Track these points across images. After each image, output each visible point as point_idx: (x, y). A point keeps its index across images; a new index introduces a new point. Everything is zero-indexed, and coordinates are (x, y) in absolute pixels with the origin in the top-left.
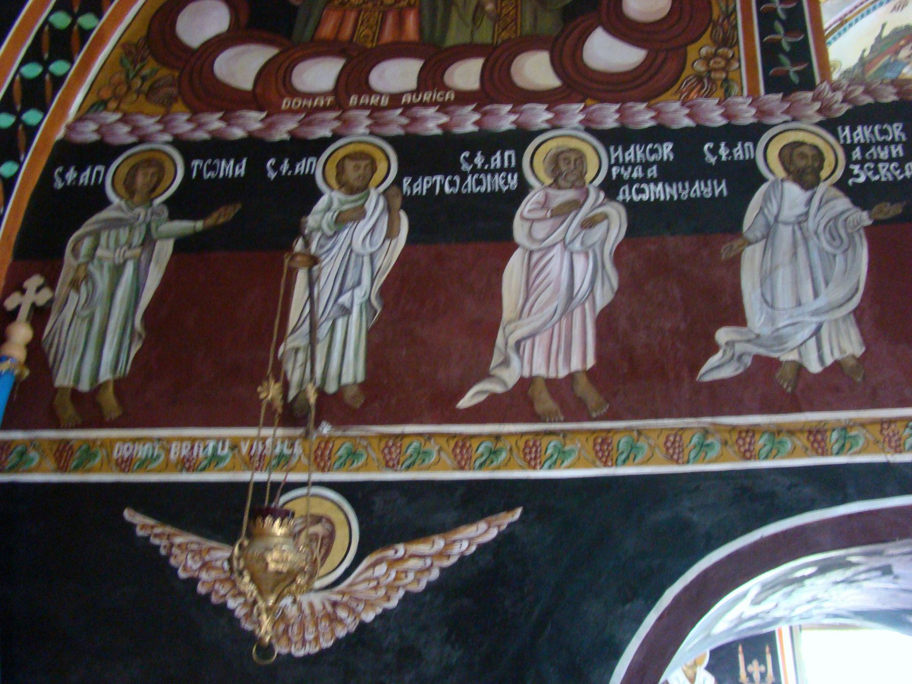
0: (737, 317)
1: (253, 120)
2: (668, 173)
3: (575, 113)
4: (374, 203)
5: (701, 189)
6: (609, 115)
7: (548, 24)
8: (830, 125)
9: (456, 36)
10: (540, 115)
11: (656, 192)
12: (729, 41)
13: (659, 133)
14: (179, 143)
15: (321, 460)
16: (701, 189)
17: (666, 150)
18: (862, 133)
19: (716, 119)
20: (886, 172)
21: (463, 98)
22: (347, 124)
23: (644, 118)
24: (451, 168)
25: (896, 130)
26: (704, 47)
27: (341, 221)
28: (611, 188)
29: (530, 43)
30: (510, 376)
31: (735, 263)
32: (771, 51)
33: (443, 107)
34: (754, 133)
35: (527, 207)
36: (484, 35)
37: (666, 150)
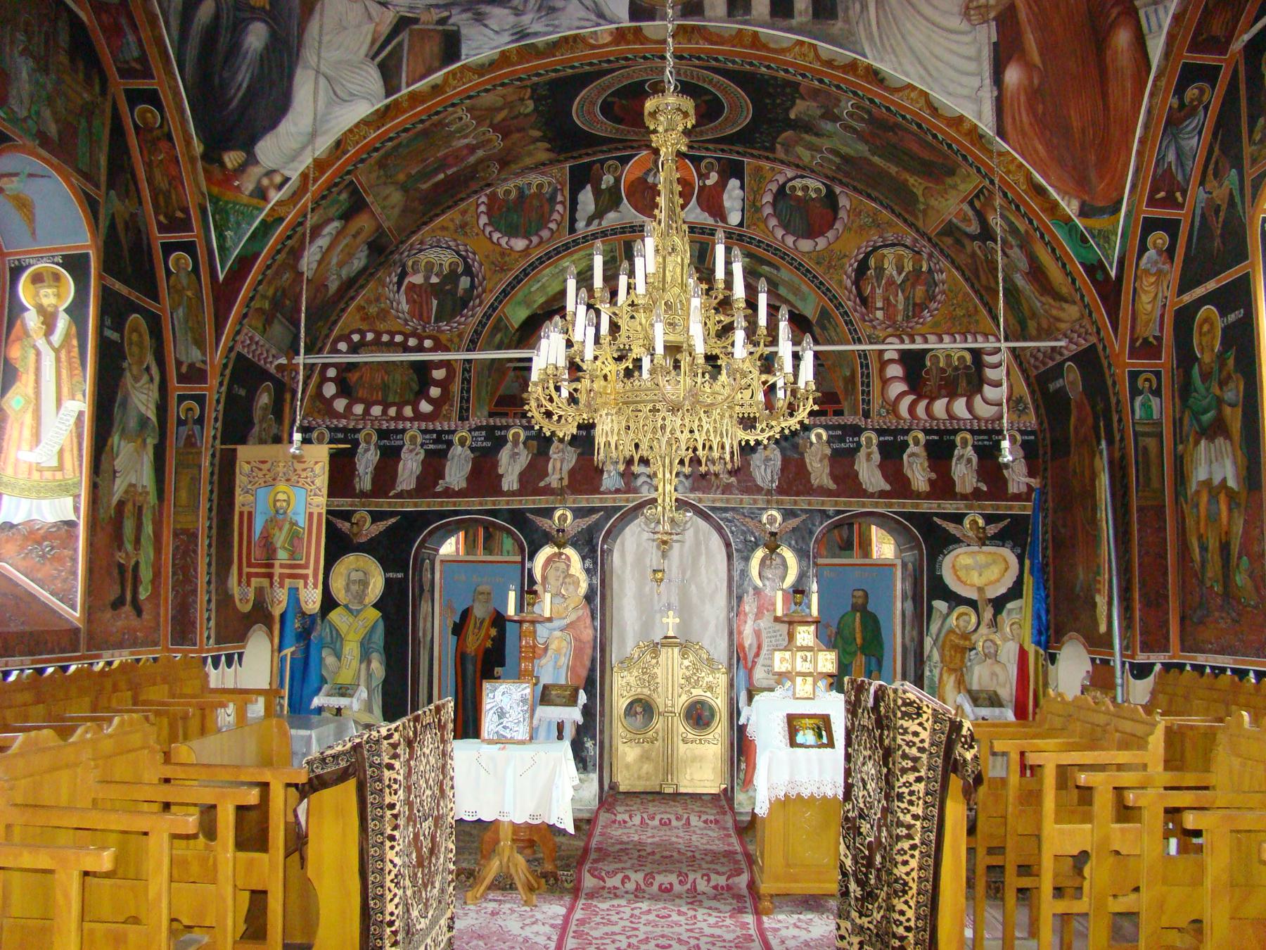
0: (443, 477)
1: (344, 422)
2: (435, 442)
3: (416, 423)
4: (372, 447)
5: (440, 447)
6: (423, 425)
7: (412, 397)
8: (470, 431)
9: (390, 399)
10: (408, 425)
11: (431, 447)
12: (452, 406)
13: (434, 431)
14: (327, 427)
15: (364, 505)
16: (440, 447)
17: (435, 436)
18: (477, 433)
19: (446, 428)
20: (479, 444)
21: (392, 419)
22: (365, 424)
23: (431, 427)
24: (388, 439)
25: (484, 433)
26: (446, 407)
27: (367, 450)
28: (422, 445)
29: (407, 403)
30: (399, 489)
31: (444, 466)
32: (461, 408)
33: (387, 421)
34: (453, 432)
35: (404, 449)
36: (397, 400)
37: (435, 436)
